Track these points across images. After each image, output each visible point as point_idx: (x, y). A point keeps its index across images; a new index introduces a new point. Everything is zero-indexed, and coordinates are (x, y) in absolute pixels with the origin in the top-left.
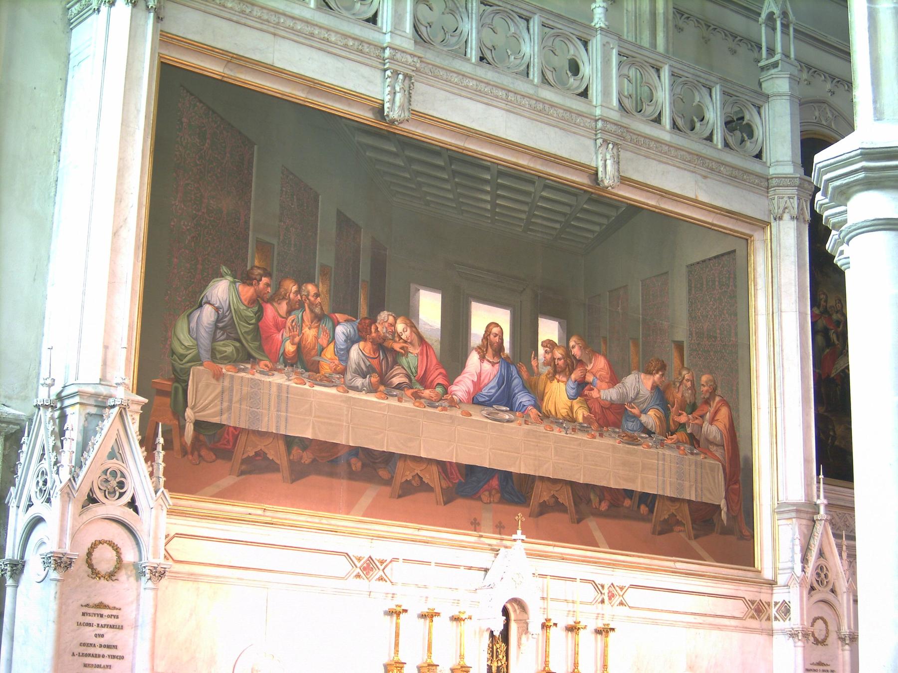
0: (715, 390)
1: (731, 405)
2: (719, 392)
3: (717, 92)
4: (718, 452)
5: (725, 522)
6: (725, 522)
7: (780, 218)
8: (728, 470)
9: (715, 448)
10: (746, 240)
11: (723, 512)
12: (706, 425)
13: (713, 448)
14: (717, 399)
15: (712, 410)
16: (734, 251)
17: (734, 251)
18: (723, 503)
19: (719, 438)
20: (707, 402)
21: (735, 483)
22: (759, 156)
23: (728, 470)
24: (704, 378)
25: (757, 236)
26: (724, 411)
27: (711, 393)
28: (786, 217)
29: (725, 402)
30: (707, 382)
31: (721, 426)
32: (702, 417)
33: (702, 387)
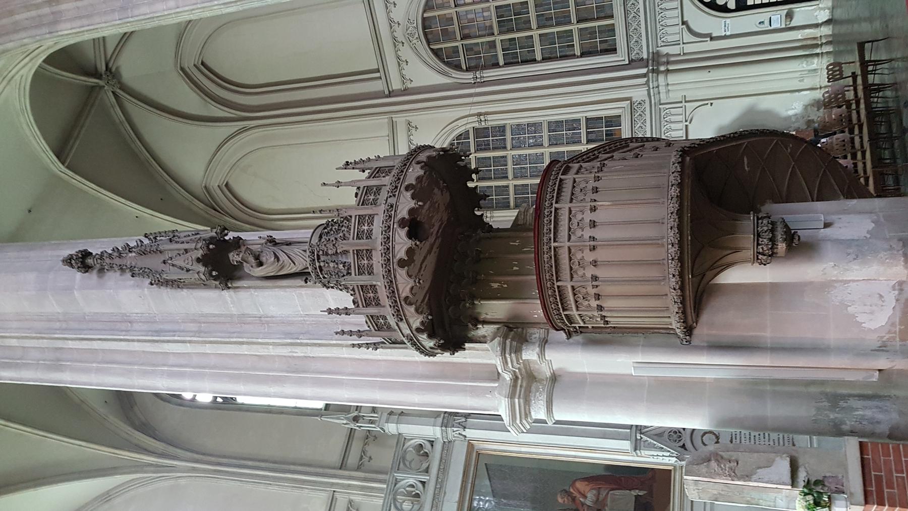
0: (566, 492)
1: (575, 478)
2: (567, 488)
3: (398, 475)
4: (603, 493)
5: (645, 492)
6: (645, 492)
7: (465, 436)
8: (614, 487)
9: (601, 496)
10: (478, 454)
11: (639, 494)
12: (588, 503)
13: (601, 497)
14: (572, 490)
15: (578, 495)
16: (486, 464)
17: (486, 464)
18: (635, 493)
19: (594, 492)
20: (574, 499)
21: (621, 480)
22: (432, 443)
23: (614, 487)
24: (560, 500)
25: (476, 448)
26: (579, 485)
27: (569, 496)
28: (464, 433)
29: (573, 484)
30: (562, 498)
31: (588, 488)
32: (583, 504)
33: (566, 503)
